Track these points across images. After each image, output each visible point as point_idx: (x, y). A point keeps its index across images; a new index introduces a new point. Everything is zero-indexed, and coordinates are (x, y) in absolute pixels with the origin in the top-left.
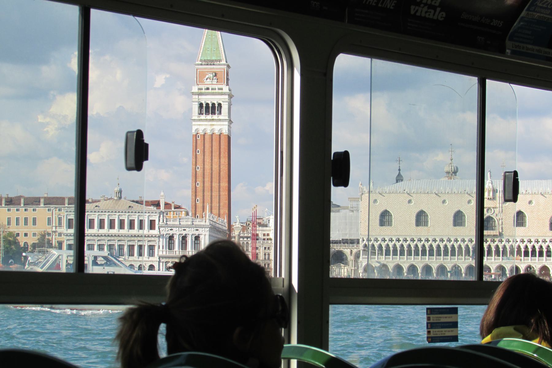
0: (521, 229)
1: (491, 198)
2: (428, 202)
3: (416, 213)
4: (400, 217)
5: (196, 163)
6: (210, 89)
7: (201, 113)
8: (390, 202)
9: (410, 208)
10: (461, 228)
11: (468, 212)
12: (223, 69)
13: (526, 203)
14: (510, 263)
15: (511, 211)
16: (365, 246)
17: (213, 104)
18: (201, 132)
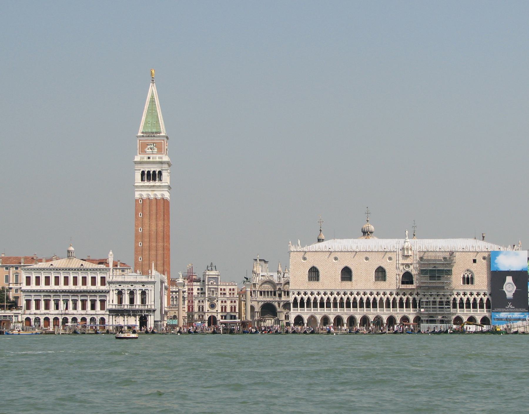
1: (408, 256)
2: (352, 259)
3: (340, 269)
4: (326, 272)
6: (151, 158)
8: (317, 260)
9: (335, 265)
10: (382, 283)
11: (388, 268)
16: (295, 299)
17: (154, 172)
18: (145, 196)
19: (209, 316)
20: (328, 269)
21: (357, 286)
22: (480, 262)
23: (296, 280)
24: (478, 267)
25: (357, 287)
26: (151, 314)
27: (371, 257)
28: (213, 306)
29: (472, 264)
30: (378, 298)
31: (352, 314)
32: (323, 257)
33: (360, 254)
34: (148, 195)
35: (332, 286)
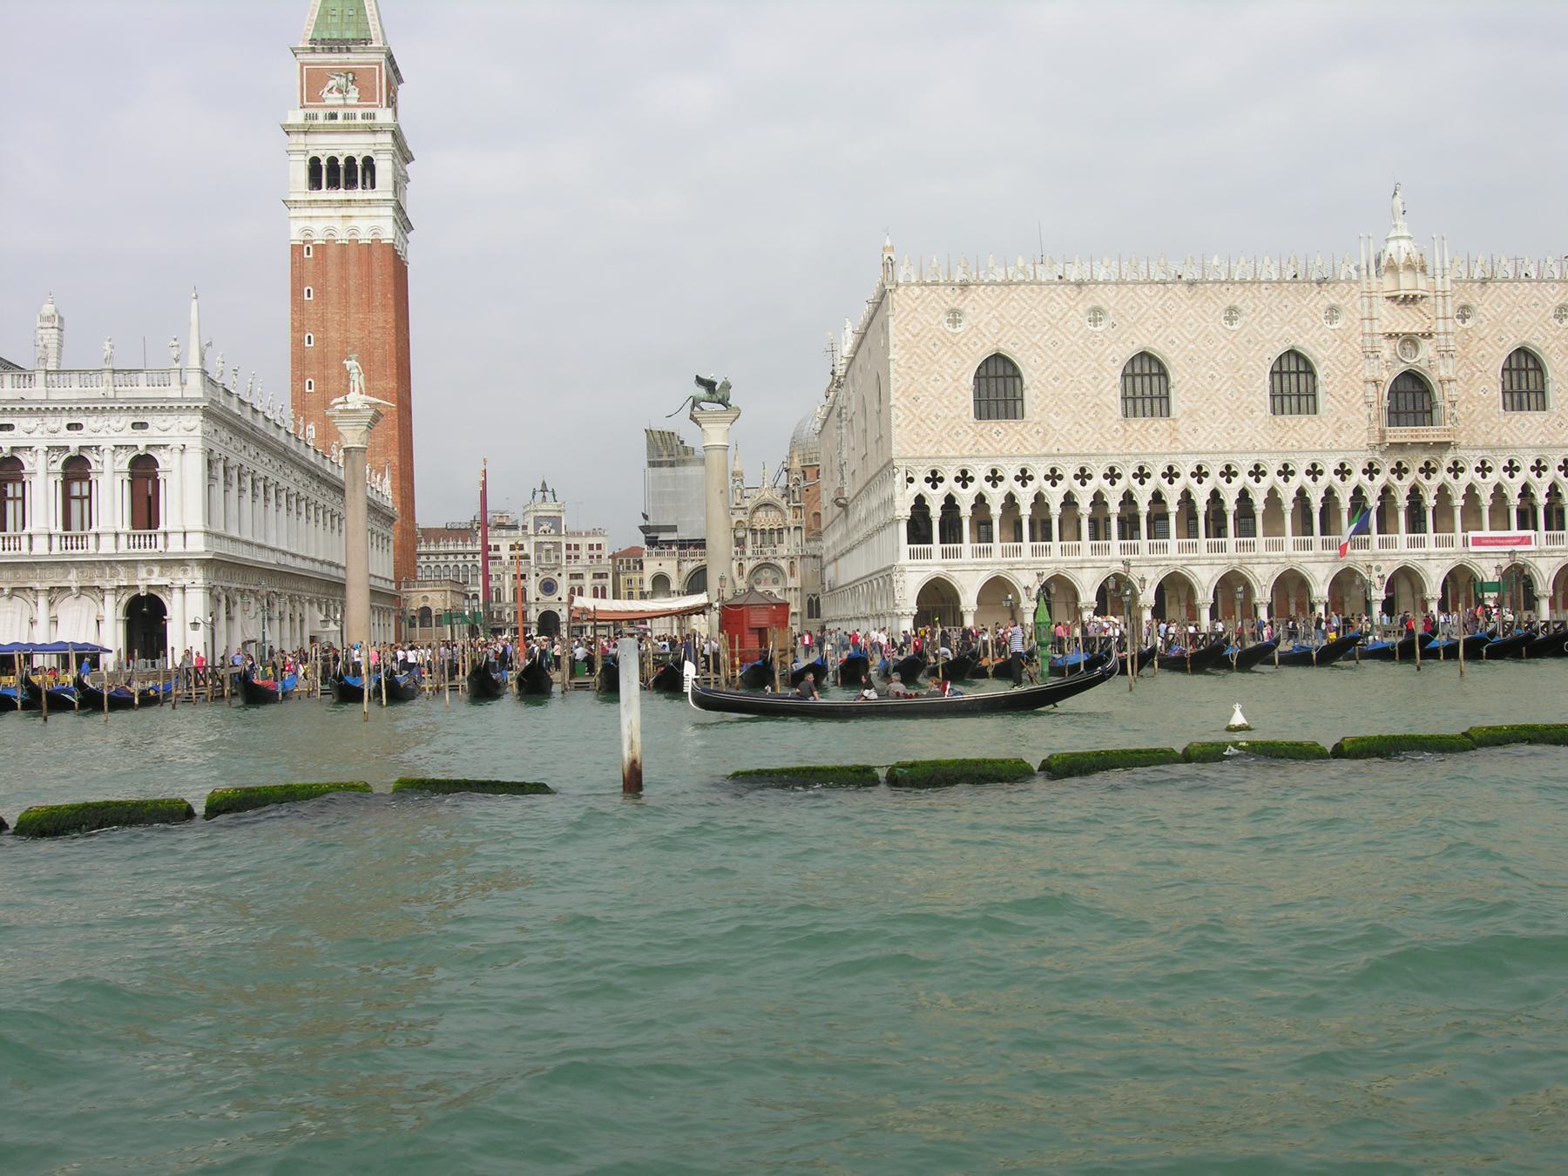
0: (1531, 419)
1: (1415, 296)
2: (1168, 318)
3: (1117, 364)
4: (1056, 379)
5: (302, 325)
6: (340, 116)
7: (315, 182)
9: (1094, 343)
11: (1326, 354)
12: (376, 64)
13: (1544, 315)
14: (1499, 555)
15: (1490, 350)
16: (920, 503)
17: (350, 161)
18: (319, 237)
19: (540, 612)
21: (1195, 439)
23: (923, 416)
25: (1196, 443)
26: (187, 582)
27: (1253, 306)
28: (548, 587)
30: (1288, 493)
33: (1202, 295)
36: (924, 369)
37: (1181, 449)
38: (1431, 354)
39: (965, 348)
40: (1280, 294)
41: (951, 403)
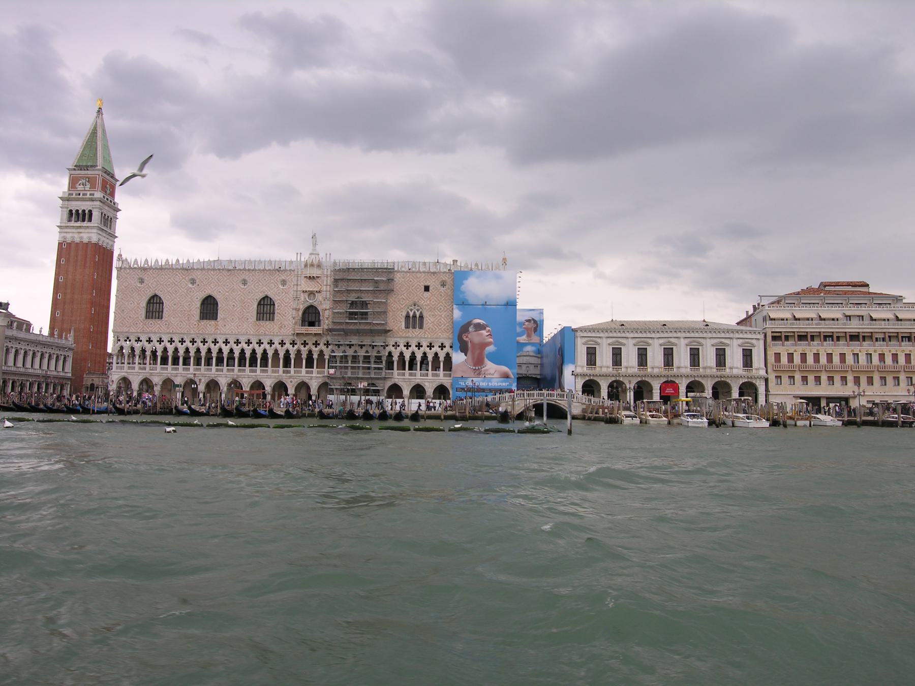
1: (313, 277)
4: (175, 305)
6: (81, 194)
7: (70, 220)
8: (161, 283)
9: (190, 292)
11: (279, 298)
17: (84, 211)
18: (69, 240)
20: (179, 298)
22: (436, 291)
24: (433, 298)
25: (225, 331)
27: (252, 279)
29: (422, 293)
30: (259, 351)
31: (213, 376)
32: (172, 279)
34: (73, 237)
35: (184, 328)
36: (127, 299)
37: (219, 332)
38: (320, 299)
39: (143, 292)
40: (263, 275)
41: (135, 312)
